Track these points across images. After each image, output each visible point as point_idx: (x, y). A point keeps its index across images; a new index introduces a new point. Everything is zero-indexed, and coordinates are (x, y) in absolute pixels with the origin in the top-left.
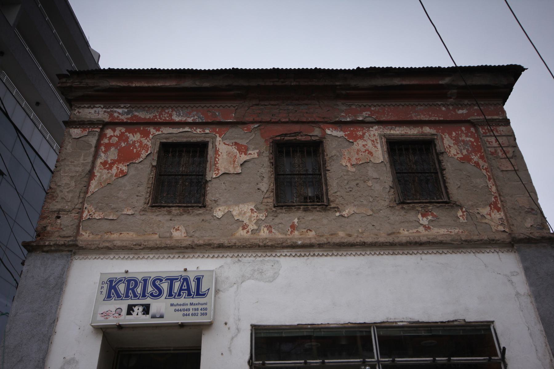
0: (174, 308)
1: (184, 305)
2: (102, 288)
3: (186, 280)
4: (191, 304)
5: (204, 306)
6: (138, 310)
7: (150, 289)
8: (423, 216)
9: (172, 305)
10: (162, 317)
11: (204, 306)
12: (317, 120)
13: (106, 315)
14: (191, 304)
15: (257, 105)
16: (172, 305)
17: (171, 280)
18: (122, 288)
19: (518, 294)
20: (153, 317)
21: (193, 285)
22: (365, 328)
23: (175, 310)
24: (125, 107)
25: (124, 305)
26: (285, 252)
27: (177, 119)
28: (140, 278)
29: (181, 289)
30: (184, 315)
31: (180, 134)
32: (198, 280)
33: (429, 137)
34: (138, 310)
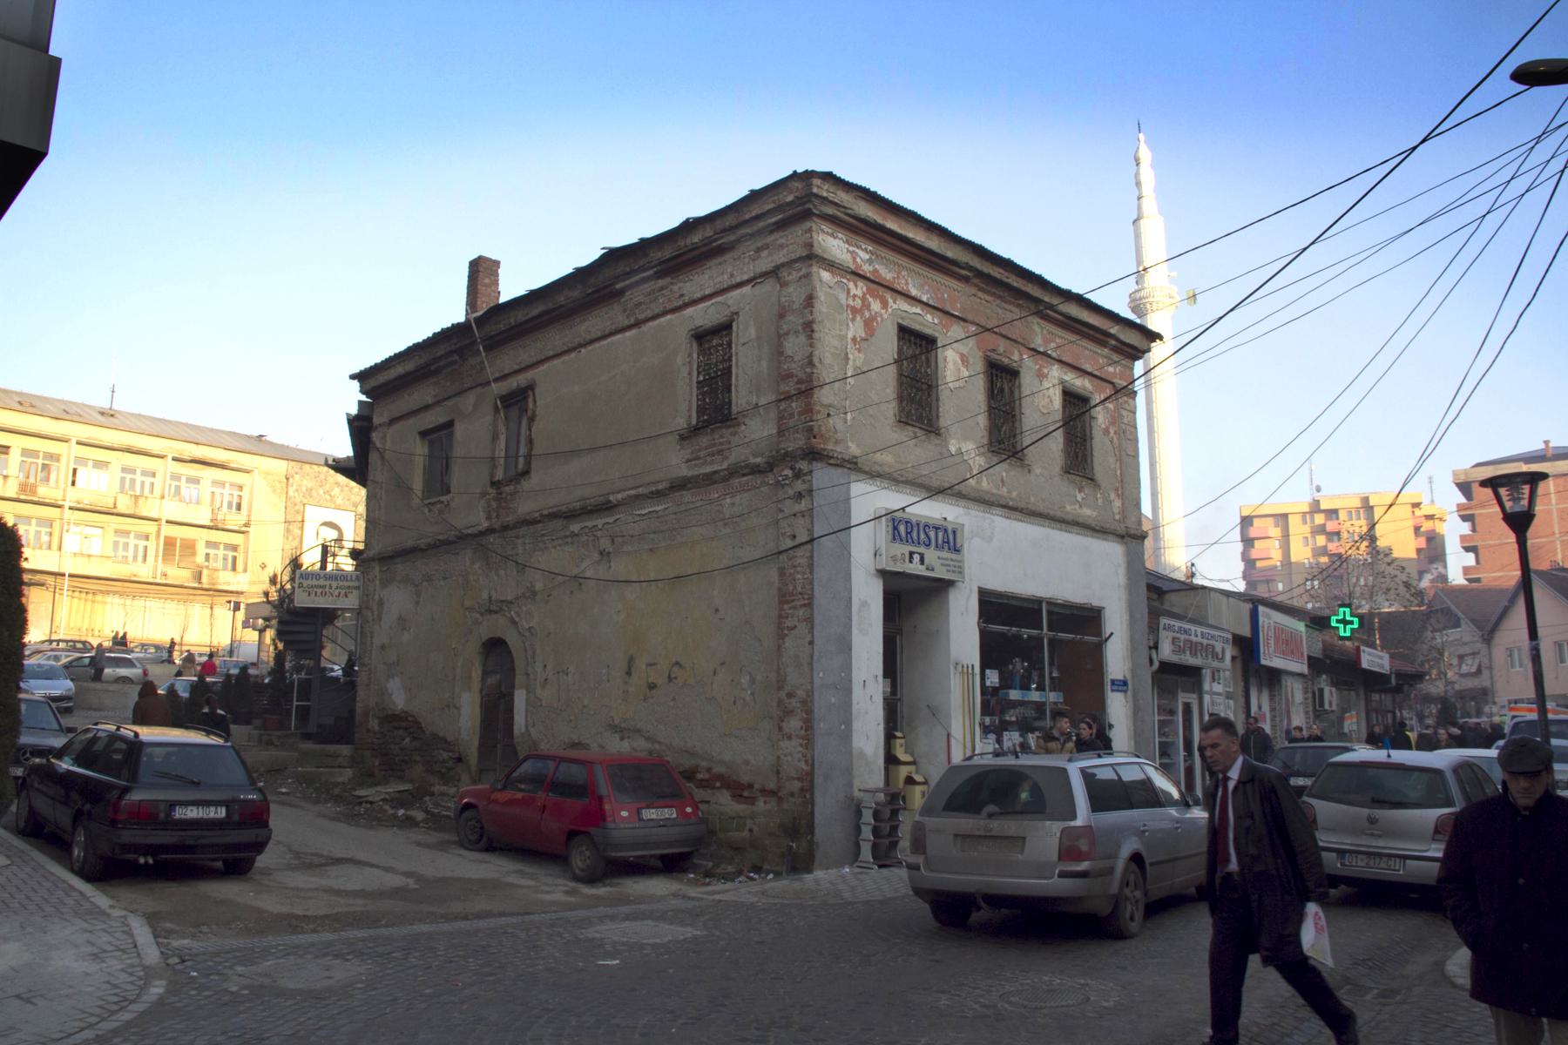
0: (940, 561)
1: (947, 559)
3: (946, 531)
4: (952, 560)
6: (916, 558)
7: (922, 536)
8: (1080, 492)
9: (939, 558)
10: (933, 570)
12: (1020, 340)
13: (894, 558)
14: (952, 560)
15: (975, 295)
16: (939, 558)
17: (937, 529)
18: (902, 528)
20: (927, 569)
21: (951, 537)
22: (1038, 601)
23: (942, 565)
24: (865, 250)
25: (907, 549)
26: (999, 511)
27: (914, 292)
28: (914, 521)
29: (944, 542)
30: (948, 571)
31: (914, 316)
33: (1087, 394)
34: (916, 558)
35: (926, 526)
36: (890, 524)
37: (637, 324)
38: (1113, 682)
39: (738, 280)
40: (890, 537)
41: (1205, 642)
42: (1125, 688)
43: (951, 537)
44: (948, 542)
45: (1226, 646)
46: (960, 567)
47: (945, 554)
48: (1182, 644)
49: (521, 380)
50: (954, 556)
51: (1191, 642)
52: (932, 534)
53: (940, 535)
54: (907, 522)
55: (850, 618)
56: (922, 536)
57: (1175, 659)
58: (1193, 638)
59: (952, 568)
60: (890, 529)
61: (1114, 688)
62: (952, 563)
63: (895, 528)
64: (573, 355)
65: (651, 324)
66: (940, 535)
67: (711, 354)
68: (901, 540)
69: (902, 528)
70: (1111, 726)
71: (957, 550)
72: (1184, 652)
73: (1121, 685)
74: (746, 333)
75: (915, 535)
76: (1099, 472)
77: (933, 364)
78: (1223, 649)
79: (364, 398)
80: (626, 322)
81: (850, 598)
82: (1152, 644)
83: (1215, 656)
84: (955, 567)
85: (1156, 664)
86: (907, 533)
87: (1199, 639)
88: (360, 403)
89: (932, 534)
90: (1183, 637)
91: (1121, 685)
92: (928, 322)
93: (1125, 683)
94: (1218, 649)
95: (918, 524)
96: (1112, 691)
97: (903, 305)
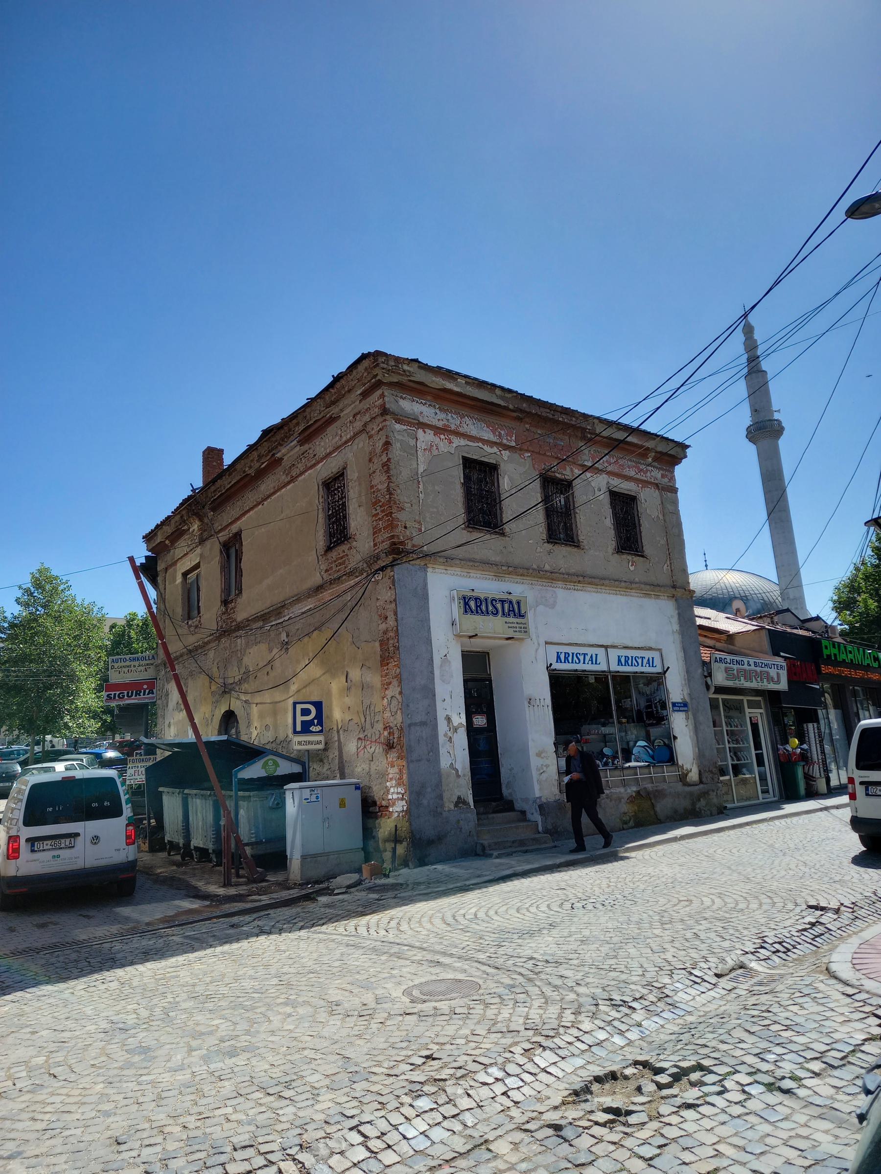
1: (513, 623)
2: (460, 603)
3: (511, 602)
5: (525, 626)
7: (490, 608)
9: (506, 623)
11: (525, 626)
16: (506, 623)
17: (503, 602)
18: (472, 604)
19: (673, 631)
21: (516, 607)
23: (509, 627)
29: (509, 611)
30: (515, 631)
32: (518, 603)
33: (633, 494)
35: (493, 600)
36: (462, 601)
37: (293, 480)
38: (674, 704)
39: (344, 439)
40: (462, 610)
41: (758, 669)
42: (686, 709)
43: (516, 607)
44: (513, 610)
45: (781, 672)
46: (526, 628)
47: (511, 619)
48: (735, 672)
49: (234, 528)
50: (520, 620)
51: (745, 670)
52: (499, 606)
53: (506, 606)
54: (476, 599)
55: (432, 673)
56: (490, 608)
57: (730, 684)
58: (746, 667)
59: (518, 629)
60: (462, 605)
61: (675, 708)
62: (518, 626)
63: (466, 604)
64: (260, 506)
65: (300, 478)
66: (506, 606)
67: (335, 494)
68: (472, 612)
69: (472, 604)
70: (675, 738)
71: (522, 616)
72: (739, 678)
73: (683, 706)
74: (352, 475)
75: (484, 608)
76: (648, 549)
77: (496, 484)
78: (778, 674)
79: (149, 554)
80: (286, 480)
81: (432, 657)
82: (706, 674)
83: (770, 679)
84: (521, 628)
85: (712, 689)
86: (477, 606)
87: (753, 667)
88: (147, 557)
89: (499, 606)
90: (735, 667)
91: (683, 706)
92: (489, 454)
93: (685, 705)
94: (773, 672)
95: (486, 600)
96: (674, 711)
97: (463, 442)
